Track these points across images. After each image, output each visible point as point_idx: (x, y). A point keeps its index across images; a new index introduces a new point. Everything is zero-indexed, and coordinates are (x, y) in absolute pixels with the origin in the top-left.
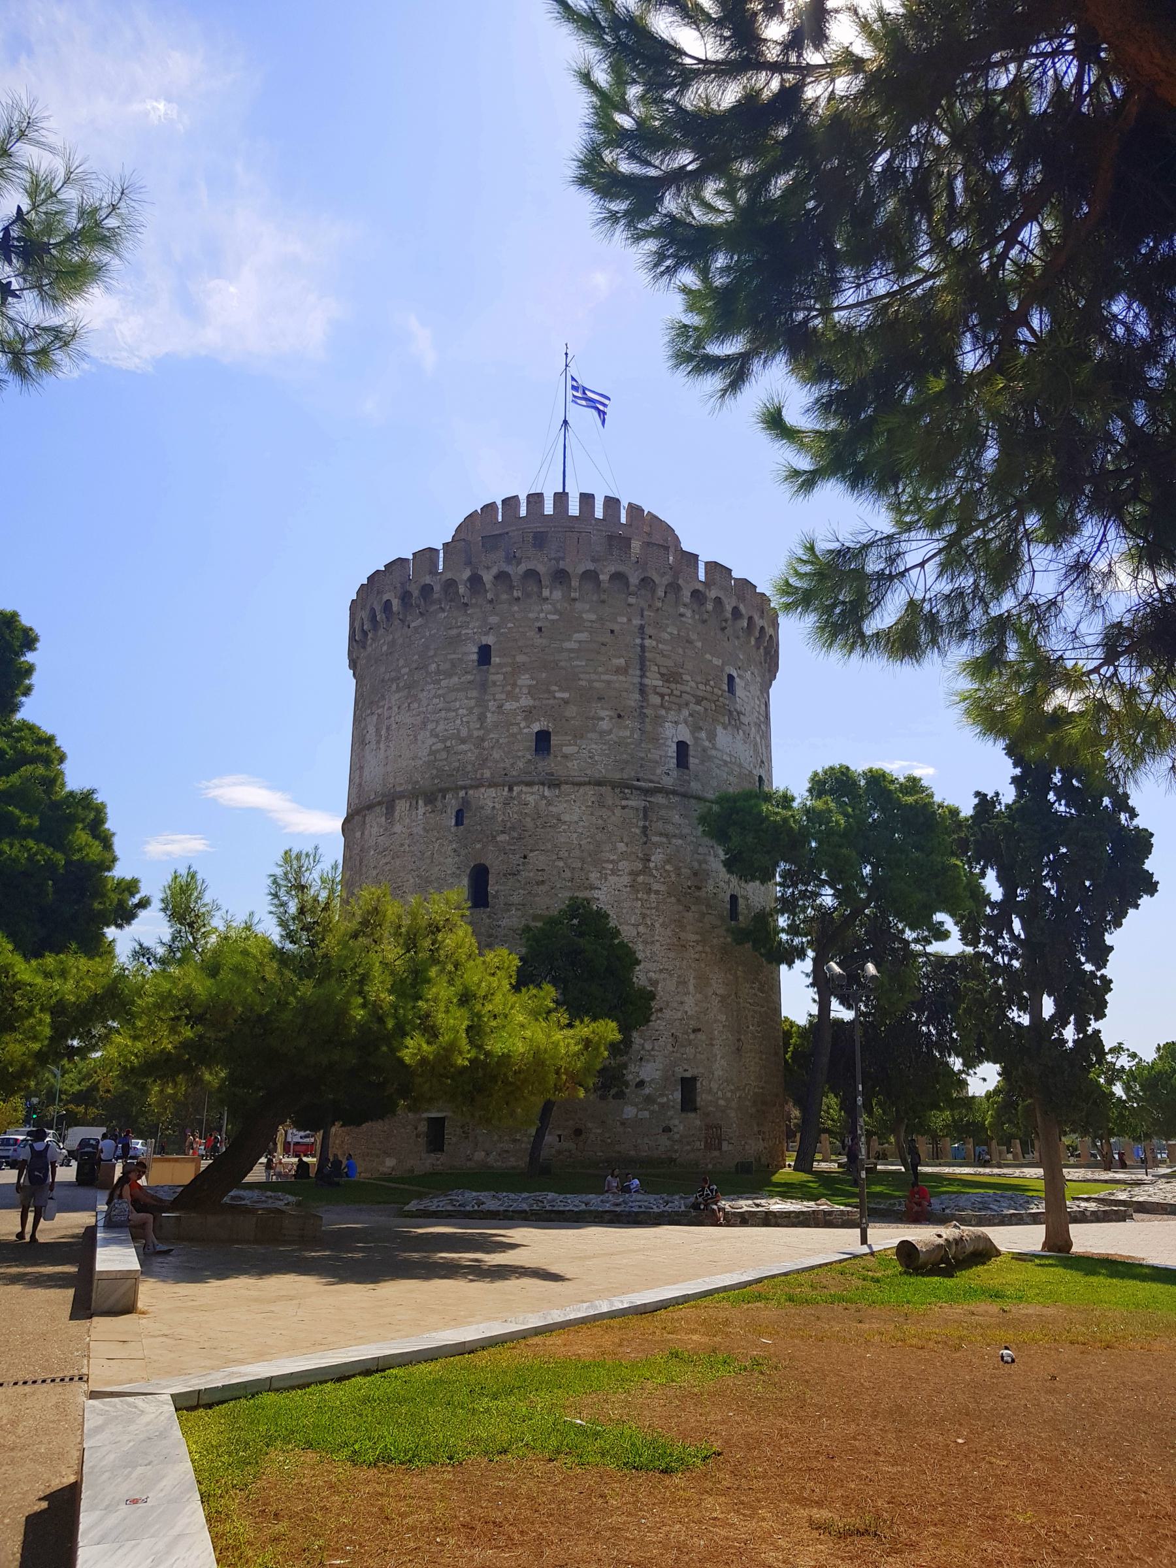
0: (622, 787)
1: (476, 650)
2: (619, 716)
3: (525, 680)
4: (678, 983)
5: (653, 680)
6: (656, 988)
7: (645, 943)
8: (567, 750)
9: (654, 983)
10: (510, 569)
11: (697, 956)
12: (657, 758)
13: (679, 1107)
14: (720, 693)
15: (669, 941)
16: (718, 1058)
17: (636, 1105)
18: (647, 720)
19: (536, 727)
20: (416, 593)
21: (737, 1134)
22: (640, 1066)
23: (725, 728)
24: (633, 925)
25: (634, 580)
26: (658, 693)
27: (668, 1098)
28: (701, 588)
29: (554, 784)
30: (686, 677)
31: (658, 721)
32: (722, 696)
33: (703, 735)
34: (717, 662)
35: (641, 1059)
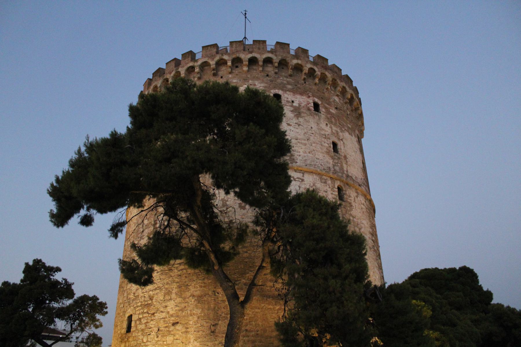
11: (179, 273)
16: (192, 341)
28: (191, 64)
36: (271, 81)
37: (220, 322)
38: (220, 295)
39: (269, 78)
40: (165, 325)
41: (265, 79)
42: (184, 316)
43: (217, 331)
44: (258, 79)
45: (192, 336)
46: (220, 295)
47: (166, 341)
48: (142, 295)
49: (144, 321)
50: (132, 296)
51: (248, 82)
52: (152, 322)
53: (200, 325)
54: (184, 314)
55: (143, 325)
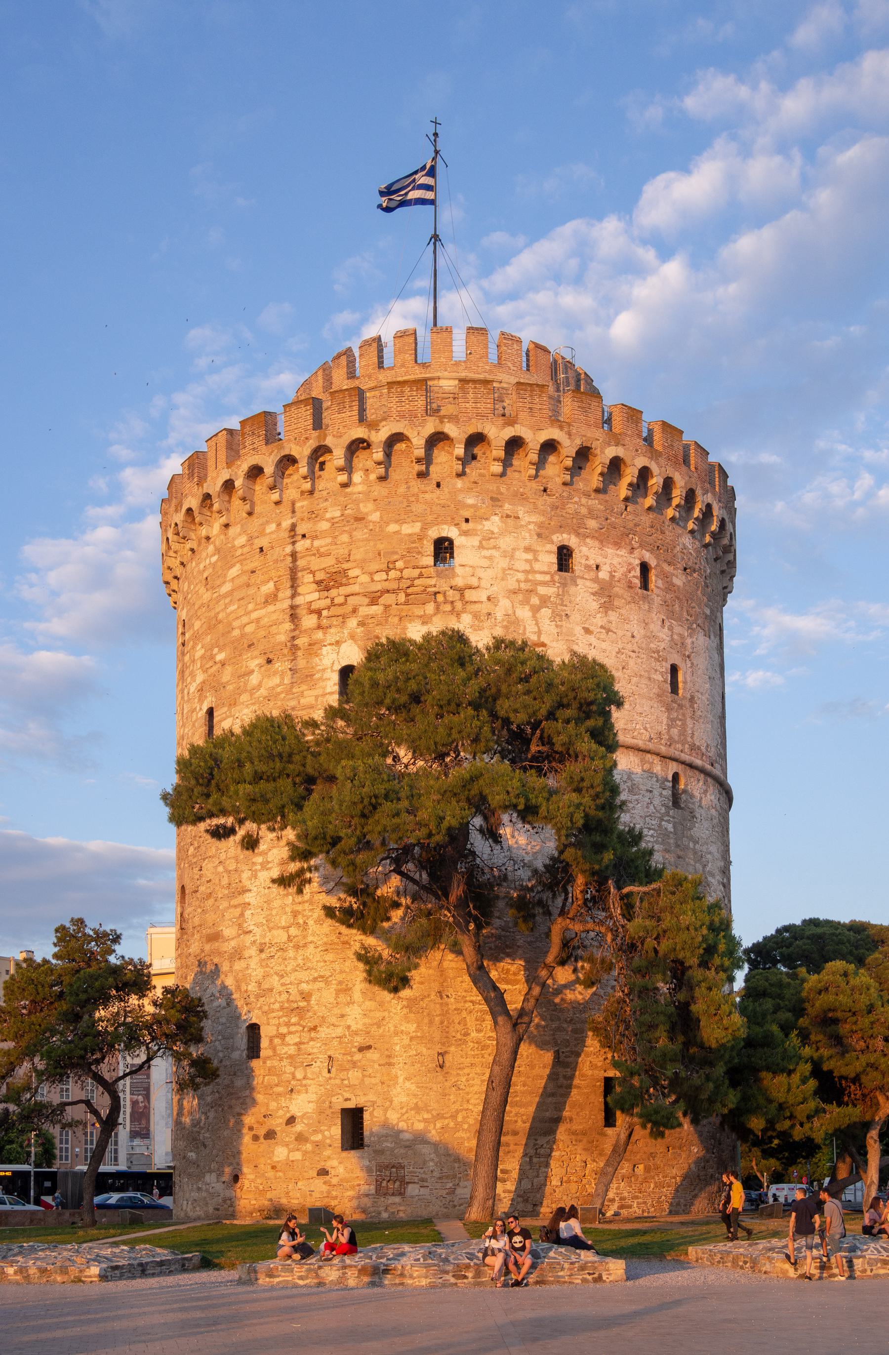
4: (338, 992)
5: (309, 594)
6: (308, 1001)
7: (297, 947)
9: (306, 996)
12: (311, 700)
13: (338, 1144)
14: (416, 572)
15: (325, 939)
16: (401, 1080)
17: (287, 1145)
18: (300, 653)
21: (436, 1174)
22: (291, 1099)
24: (283, 928)
26: (312, 612)
27: (324, 1136)
30: (351, 573)
31: (313, 648)
32: (421, 576)
35: (292, 1090)
36: (555, 507)
37: (453, 1049)
38: (452, 1000)
39: (549, 500)
40: (343, 1052)
41: (540, 503)
42: (382, 1036)
43: (447, 1064)
44: (522, 498)
45: (399, 1073)
46: (452, 1000)
47: (348, 1079)
48: (281, 989)
49: (292, 1039)
50: (252, 987)
51: (501, 506)
52: (311, 1043)
53: (414, 1052)
54: (381, 1031)
55: (292, 1047)
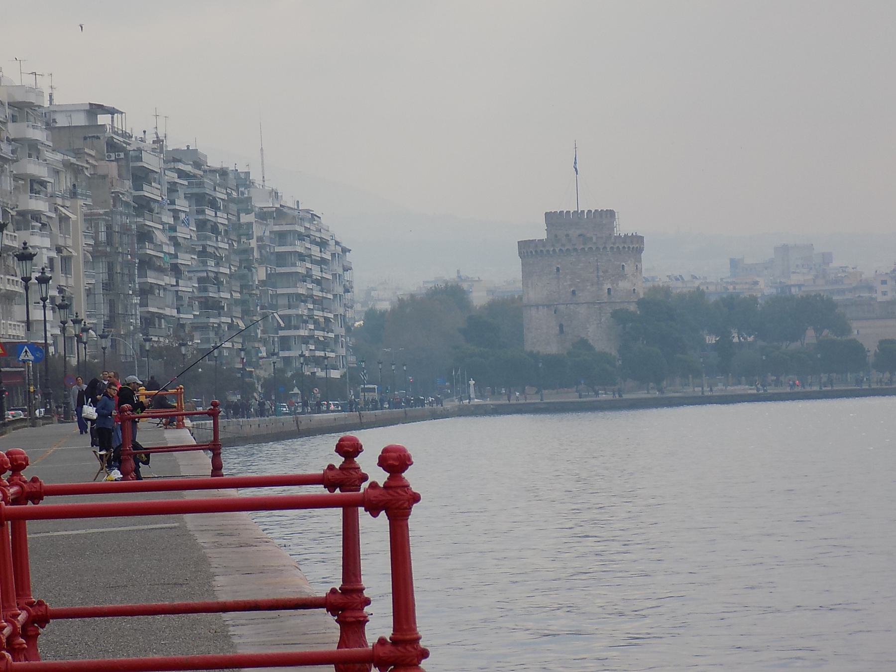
0: (594, 303)
1: (555, 268)
2: (593, 285)
3: (568, 277)
5: (601, 274)
8: (580, 295)
10: (563, 249)
19: (572, 289)
20: (539, 251)
23: (621, 280)
25: (594, 249)
28: (612, 245)
29: (578, 304)
30: (610, 270)
33: (615, 285)
34: (618, 263)
